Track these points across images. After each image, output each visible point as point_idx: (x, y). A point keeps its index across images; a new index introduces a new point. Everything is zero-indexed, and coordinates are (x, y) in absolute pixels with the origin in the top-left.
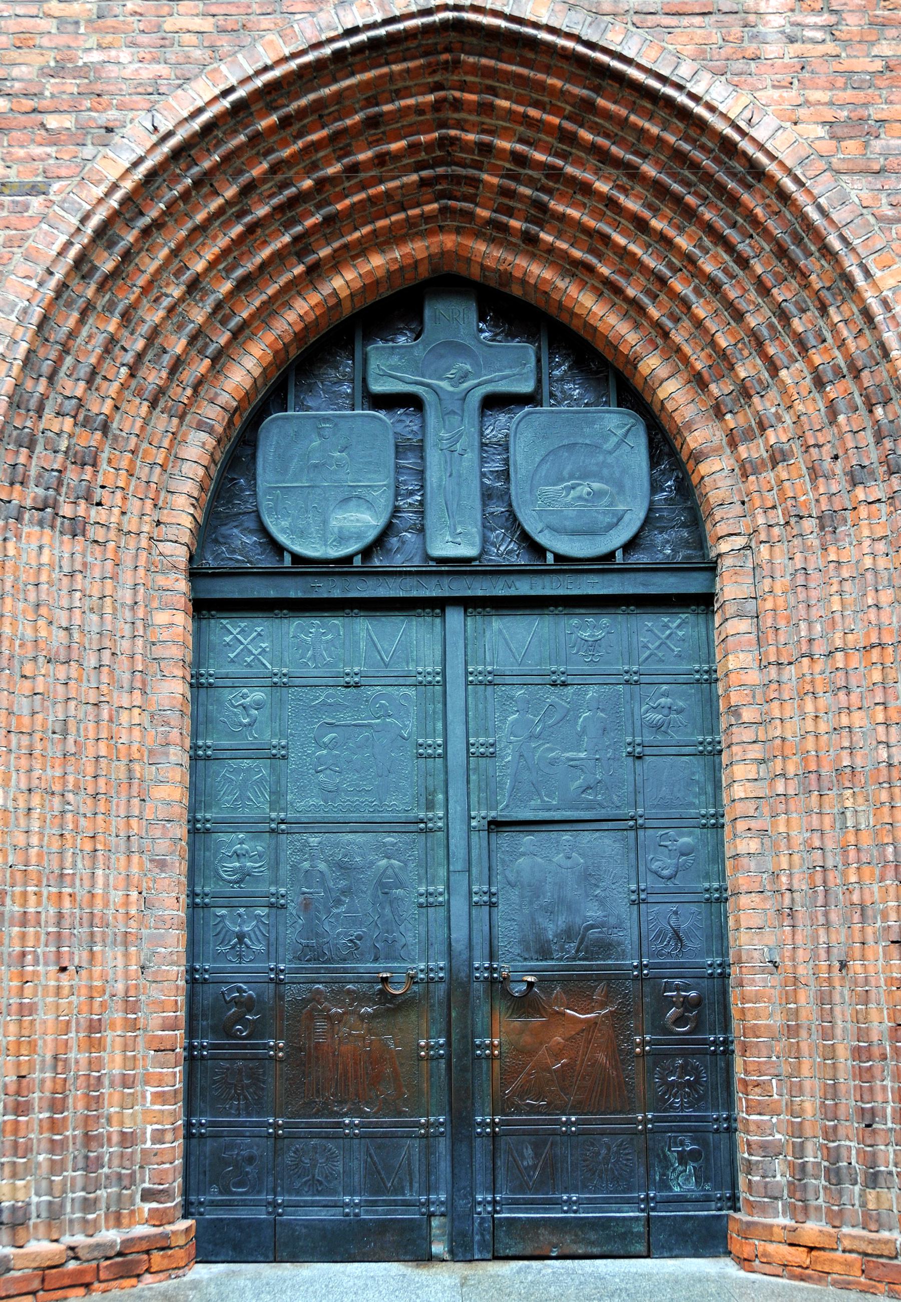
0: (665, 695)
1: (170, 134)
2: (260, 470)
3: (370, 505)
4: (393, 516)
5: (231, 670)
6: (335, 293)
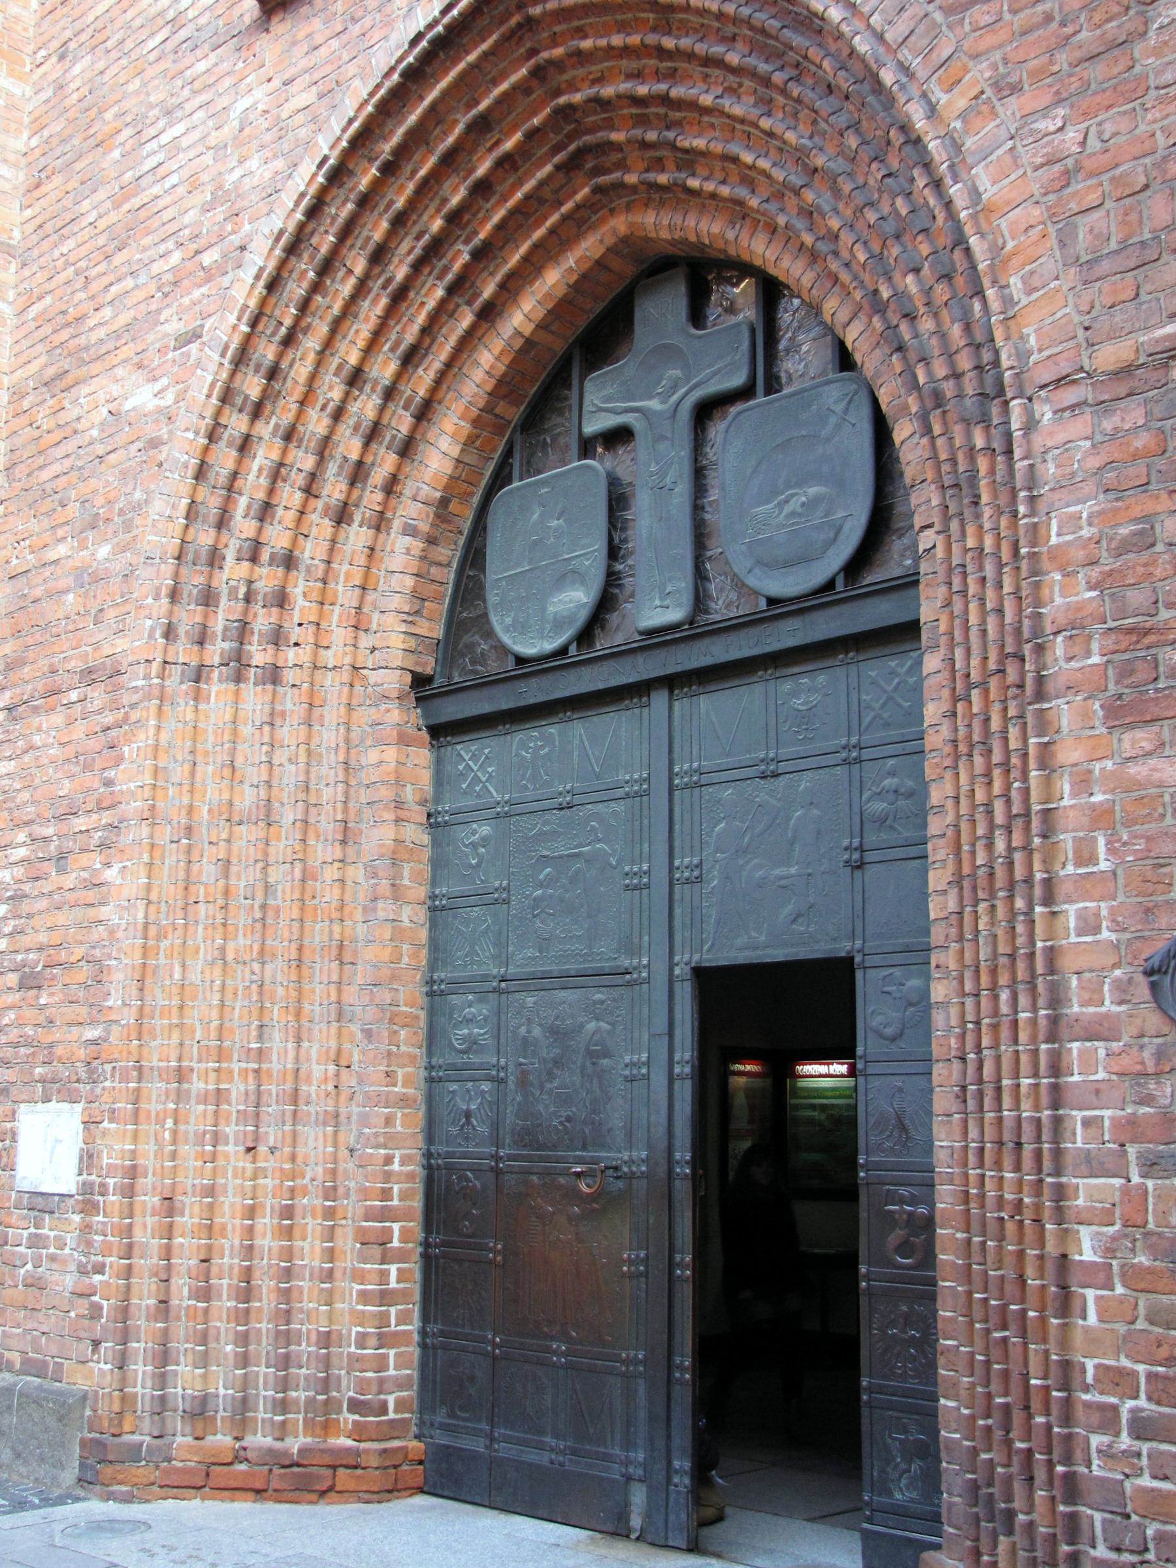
0: (892, 773)
6: (518, 333)
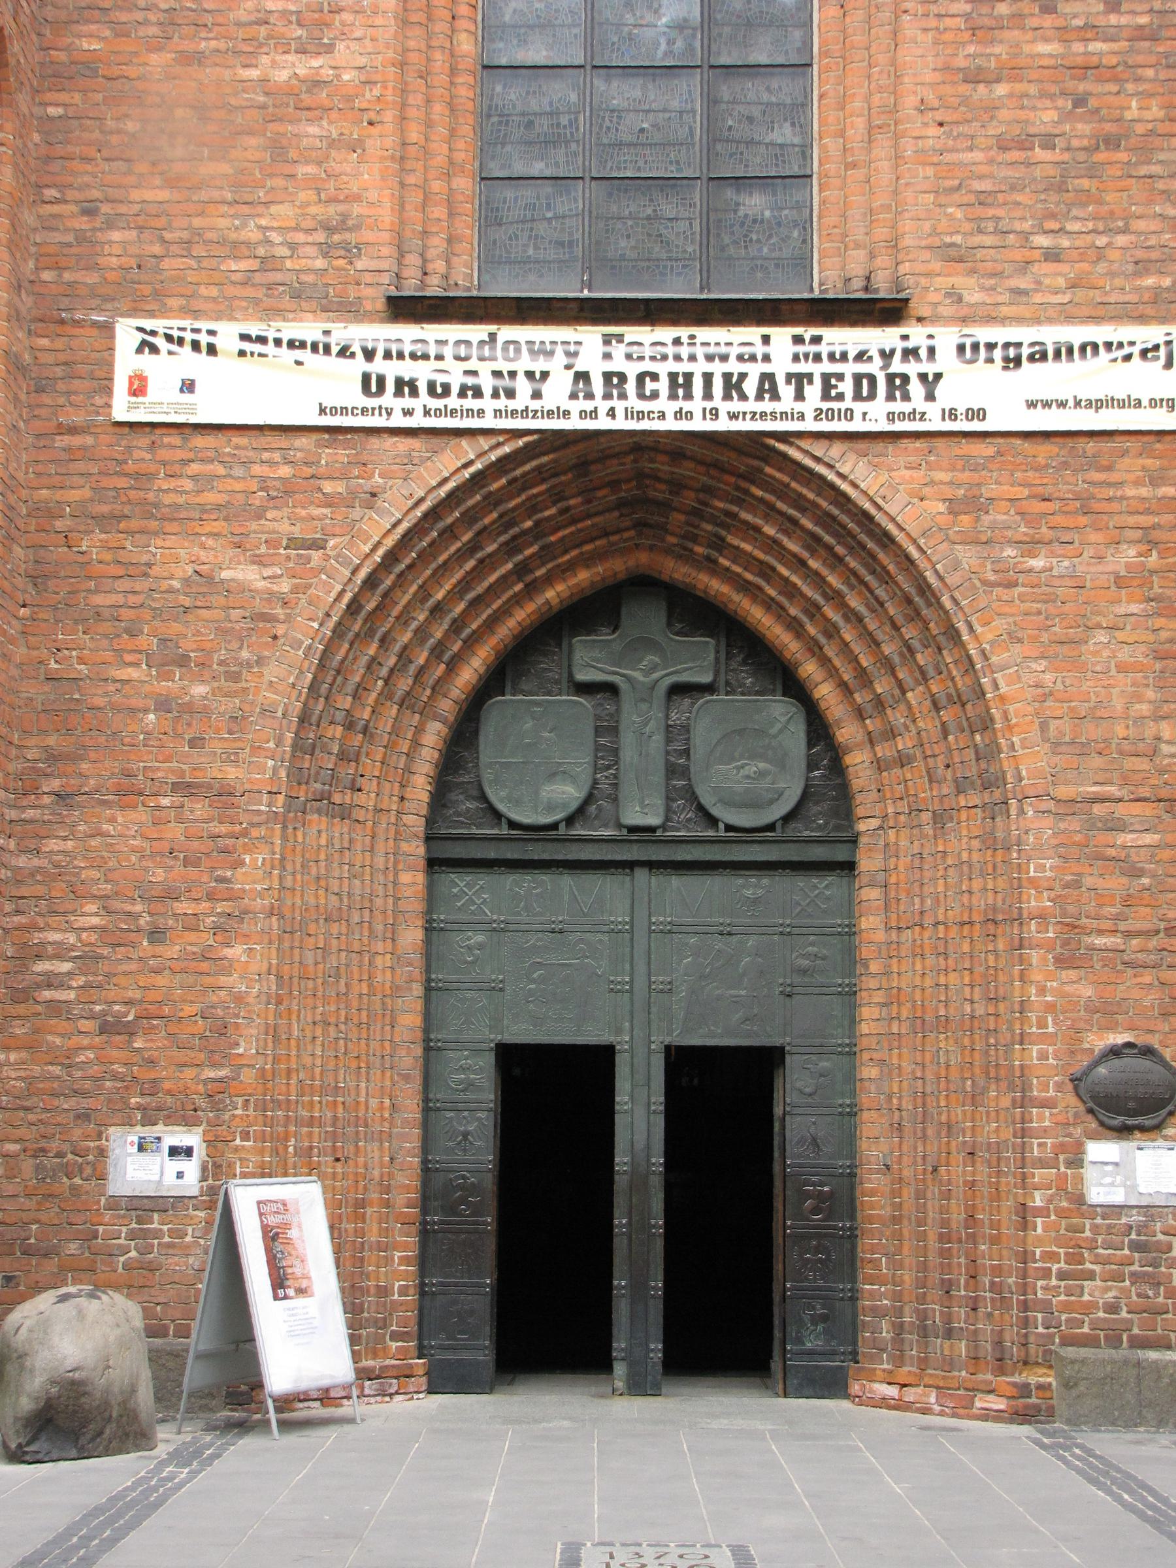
0: (812, 944)
1: (421, 500)
2: (482, 747)
3: (574, 780)
5: (460, 917)
6: (547, 602)
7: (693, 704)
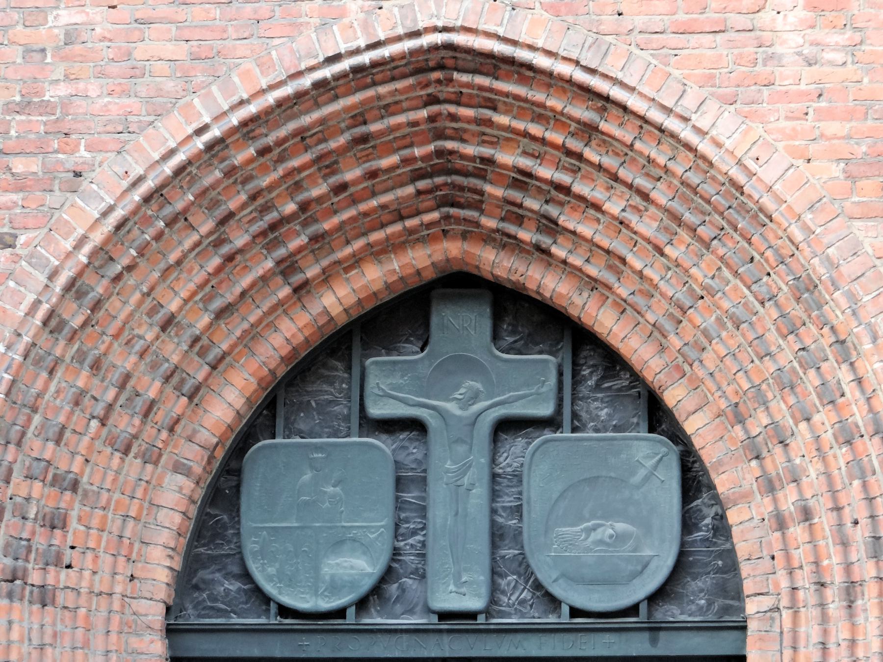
1: (140, 180)
2: (243, 508)
3: (366, 549)
4: (393, 560)
6: (326, 311)
7: (529, 443)
